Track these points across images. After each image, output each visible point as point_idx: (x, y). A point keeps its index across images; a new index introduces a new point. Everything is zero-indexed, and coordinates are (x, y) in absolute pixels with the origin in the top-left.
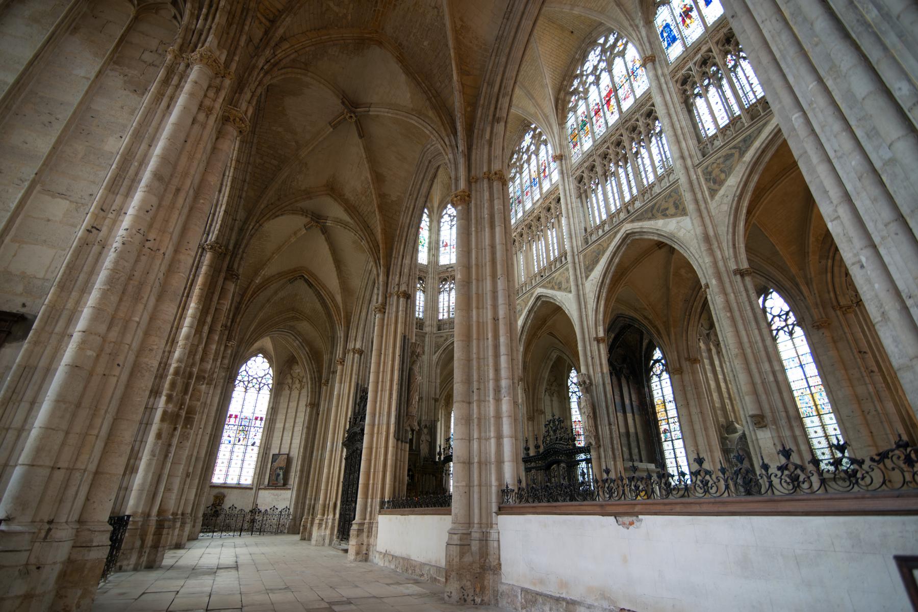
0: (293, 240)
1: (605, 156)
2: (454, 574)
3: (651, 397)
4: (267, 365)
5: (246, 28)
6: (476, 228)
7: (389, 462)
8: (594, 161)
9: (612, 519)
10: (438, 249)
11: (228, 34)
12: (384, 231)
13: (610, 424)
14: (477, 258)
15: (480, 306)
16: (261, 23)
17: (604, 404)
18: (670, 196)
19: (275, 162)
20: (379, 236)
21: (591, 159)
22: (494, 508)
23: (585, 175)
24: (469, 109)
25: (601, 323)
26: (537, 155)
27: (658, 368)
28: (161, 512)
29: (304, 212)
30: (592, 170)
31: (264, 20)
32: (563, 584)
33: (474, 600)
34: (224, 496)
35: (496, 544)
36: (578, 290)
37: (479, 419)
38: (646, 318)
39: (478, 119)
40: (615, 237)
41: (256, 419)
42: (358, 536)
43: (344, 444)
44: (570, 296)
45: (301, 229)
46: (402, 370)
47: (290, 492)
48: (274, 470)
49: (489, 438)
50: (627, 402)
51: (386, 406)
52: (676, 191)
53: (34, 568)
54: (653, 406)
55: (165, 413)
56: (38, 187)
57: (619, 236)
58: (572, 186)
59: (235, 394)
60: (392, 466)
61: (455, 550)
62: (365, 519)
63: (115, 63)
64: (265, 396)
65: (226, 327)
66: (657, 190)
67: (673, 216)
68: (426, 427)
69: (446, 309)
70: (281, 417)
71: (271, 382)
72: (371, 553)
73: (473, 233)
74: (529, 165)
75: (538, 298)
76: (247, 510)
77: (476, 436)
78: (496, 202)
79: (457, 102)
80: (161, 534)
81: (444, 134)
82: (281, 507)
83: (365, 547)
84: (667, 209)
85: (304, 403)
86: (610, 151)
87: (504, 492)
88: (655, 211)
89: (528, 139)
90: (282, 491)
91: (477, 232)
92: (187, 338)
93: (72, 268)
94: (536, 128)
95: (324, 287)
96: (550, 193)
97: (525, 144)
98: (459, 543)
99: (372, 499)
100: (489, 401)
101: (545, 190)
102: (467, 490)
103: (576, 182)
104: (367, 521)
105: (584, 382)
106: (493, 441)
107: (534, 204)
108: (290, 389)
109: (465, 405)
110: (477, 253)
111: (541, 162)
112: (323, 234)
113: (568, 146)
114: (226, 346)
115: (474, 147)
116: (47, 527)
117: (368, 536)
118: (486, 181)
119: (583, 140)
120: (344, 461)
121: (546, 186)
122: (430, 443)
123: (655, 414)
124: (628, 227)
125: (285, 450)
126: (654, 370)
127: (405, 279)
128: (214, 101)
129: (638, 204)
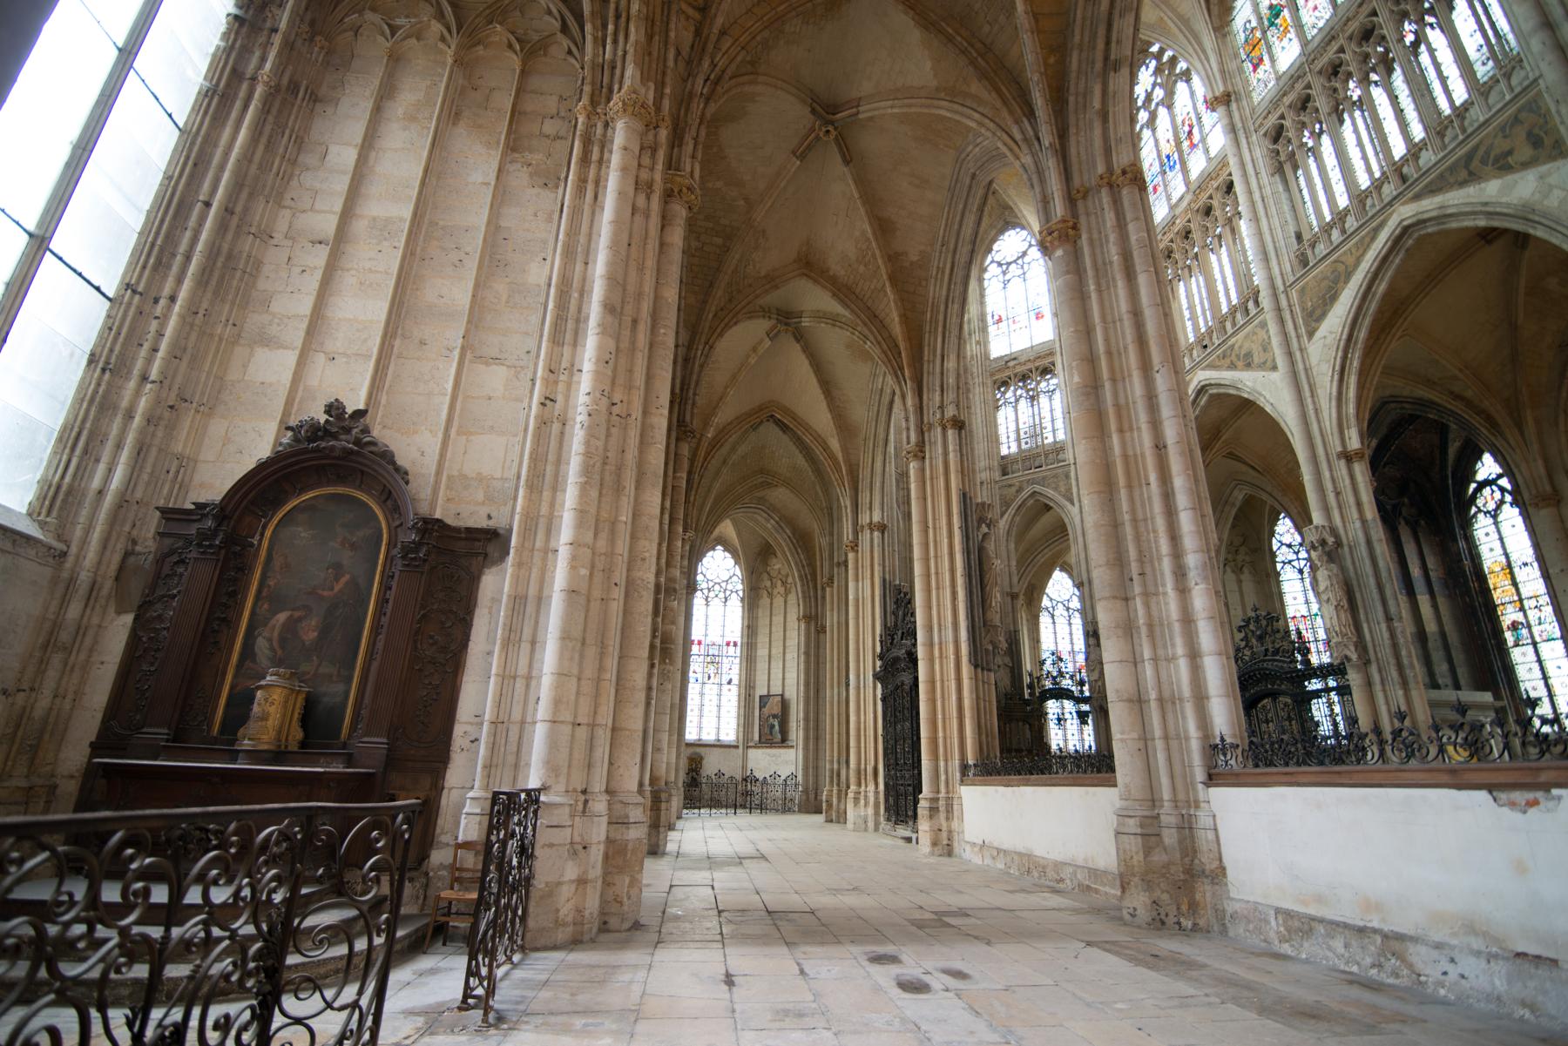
0: (752, 361)
1: (1335, 71)
2: (1136, 879)
3: (1476, 558)
5: (672, 34)
6: (1098, 285)
7: (967, 703)
8: (1308, 86)
9: (1482, 795)
11: (650, 54)
12: (905, 319)
13: (1389, 619)
14: (1107, 340)
15: (1126, 426)
16: (688, 18)
17: (1372, 581)
18: (1516, 120)
19: (719, 241)
20: (897, 329)
21: (1299, 86)
22: (1200, 775)
23: (1287, 123)
24: (1052, 60)
25: (1353, 420)
26: (1170, 107)
27: (1488, 498)
28: (653, 780)
29: (765, 312)
30: (1304, 108)
31: (690, 11)
32: (1370, 906)
33: (1179, 923)
35: (1211, 835)
36: (1292, 363)
37: (1150, 626)
38: (1458, 397)
39: (1073, 75)
40: (1373, 239)
41: (728, 644)
42: (931, 817)
43: (876, 677)
44: (1275, 376)
45: (762, 341)
46: (967, 552)
47: (792, 751)
48: (767, 722)
49: (1174, 658)
50: (1416, 572)
52: (1535, 106)
53: (580, 847)
54: (1481, 577)
56: (469, 356)
57: (1383, 236)
58: (1258, 151)
61: (1134, 845)
63: (514, 150)
64: (735, 610)
66: (1478, 114)
67: (1525, 165)
69: (1013, 436)
70: (762, 639)
71: (740, 587)
72: (956, 844)
73: (1094, 296)
74: (1154, 130)
75: (1201, 390)
77: (1147, 654)
78: (1131, 227)
79: (1029, 54)
80: (659, 809)
81: (1009, 121)
82: (785, 772)
83: (944, 835)
84: (1510, 153)
86: (1347, 57)
87: (1214, 749)
88: (1475, 163)
89: (1145, 78)
91: (1099, 291)
93: (537, 459)
94: (1162, 51)
95: (808, 428)
96: (1207, 177)
97: (1140, 91)
98: (1139, 831)
99: (946, 761)
100: (1165, 594)
101: (1194, 174)
102: (1141, 745)
103: (1267, 143)
105: (1323, 542)
106: (1183, 665)
107: (1172, 208)
108: (770, 595)
109: (1119, 604)
110: (1106, 331)
111: (1179, 120)
112: (798, 341)
113: (1241, 71)
115: (1072, 130)
116: (582, 798)
117: (947, 819)
118: (1104, 192)
119: (1277, 49)
120: (880, 704)
121: (1197, 164)
122: (1012, 670)
123: (1486, 592)
124: (1406, 212)
125: (776, 690)
126: (1480, 502)
127: (950, 396)
128: (652, 169)
129: (1428, 158)
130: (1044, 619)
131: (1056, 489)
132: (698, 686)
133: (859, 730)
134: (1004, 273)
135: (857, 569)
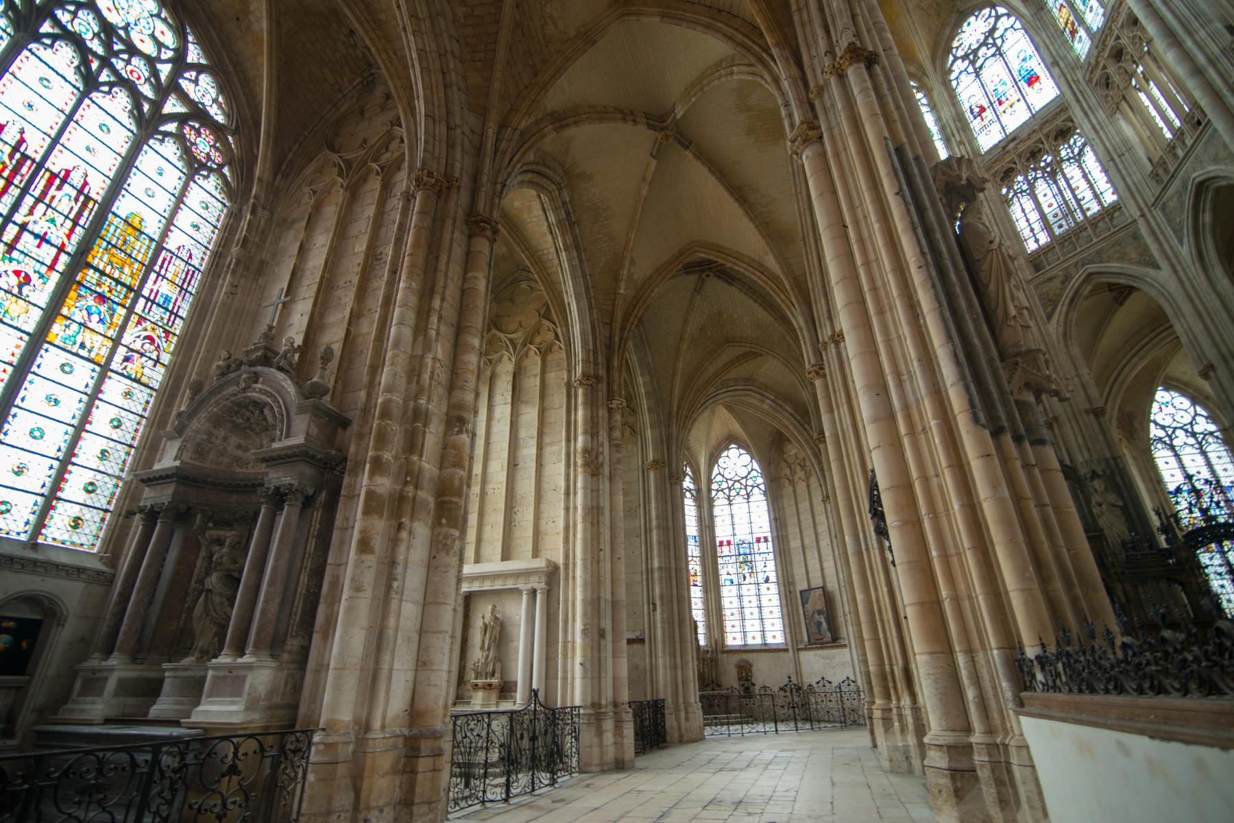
4: (746, 458)
10: (964, 127)
34: (751, 666)
47: (846, 650)
48: (815, 618)
51: (909, 344)
55: (370, 495)
59: (716, 511)
60: (1005, 521)
62: (968, 729)
65: (597, 377)
68: (1094, 475)
70: (793, 530)
71: (760, 480)
76: (776, 689)
82: (837, 676)
85: (820, 498)
90: (835, 651)
92: (397, 344)
99: (970, 652)
104: (977, 738)
108: (792, 482)
112: (687, 148)
114: (610, 410)
117: (1003, 802)
122: (1125, 510)
125: (817, 582)
130: (1162, 456)
131: (1122, 258)
132: (734, 588)
133: (871, 613)
134: (973, 63)
135: (828, 397)
